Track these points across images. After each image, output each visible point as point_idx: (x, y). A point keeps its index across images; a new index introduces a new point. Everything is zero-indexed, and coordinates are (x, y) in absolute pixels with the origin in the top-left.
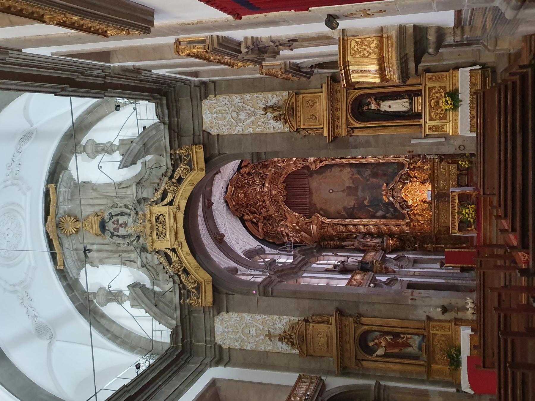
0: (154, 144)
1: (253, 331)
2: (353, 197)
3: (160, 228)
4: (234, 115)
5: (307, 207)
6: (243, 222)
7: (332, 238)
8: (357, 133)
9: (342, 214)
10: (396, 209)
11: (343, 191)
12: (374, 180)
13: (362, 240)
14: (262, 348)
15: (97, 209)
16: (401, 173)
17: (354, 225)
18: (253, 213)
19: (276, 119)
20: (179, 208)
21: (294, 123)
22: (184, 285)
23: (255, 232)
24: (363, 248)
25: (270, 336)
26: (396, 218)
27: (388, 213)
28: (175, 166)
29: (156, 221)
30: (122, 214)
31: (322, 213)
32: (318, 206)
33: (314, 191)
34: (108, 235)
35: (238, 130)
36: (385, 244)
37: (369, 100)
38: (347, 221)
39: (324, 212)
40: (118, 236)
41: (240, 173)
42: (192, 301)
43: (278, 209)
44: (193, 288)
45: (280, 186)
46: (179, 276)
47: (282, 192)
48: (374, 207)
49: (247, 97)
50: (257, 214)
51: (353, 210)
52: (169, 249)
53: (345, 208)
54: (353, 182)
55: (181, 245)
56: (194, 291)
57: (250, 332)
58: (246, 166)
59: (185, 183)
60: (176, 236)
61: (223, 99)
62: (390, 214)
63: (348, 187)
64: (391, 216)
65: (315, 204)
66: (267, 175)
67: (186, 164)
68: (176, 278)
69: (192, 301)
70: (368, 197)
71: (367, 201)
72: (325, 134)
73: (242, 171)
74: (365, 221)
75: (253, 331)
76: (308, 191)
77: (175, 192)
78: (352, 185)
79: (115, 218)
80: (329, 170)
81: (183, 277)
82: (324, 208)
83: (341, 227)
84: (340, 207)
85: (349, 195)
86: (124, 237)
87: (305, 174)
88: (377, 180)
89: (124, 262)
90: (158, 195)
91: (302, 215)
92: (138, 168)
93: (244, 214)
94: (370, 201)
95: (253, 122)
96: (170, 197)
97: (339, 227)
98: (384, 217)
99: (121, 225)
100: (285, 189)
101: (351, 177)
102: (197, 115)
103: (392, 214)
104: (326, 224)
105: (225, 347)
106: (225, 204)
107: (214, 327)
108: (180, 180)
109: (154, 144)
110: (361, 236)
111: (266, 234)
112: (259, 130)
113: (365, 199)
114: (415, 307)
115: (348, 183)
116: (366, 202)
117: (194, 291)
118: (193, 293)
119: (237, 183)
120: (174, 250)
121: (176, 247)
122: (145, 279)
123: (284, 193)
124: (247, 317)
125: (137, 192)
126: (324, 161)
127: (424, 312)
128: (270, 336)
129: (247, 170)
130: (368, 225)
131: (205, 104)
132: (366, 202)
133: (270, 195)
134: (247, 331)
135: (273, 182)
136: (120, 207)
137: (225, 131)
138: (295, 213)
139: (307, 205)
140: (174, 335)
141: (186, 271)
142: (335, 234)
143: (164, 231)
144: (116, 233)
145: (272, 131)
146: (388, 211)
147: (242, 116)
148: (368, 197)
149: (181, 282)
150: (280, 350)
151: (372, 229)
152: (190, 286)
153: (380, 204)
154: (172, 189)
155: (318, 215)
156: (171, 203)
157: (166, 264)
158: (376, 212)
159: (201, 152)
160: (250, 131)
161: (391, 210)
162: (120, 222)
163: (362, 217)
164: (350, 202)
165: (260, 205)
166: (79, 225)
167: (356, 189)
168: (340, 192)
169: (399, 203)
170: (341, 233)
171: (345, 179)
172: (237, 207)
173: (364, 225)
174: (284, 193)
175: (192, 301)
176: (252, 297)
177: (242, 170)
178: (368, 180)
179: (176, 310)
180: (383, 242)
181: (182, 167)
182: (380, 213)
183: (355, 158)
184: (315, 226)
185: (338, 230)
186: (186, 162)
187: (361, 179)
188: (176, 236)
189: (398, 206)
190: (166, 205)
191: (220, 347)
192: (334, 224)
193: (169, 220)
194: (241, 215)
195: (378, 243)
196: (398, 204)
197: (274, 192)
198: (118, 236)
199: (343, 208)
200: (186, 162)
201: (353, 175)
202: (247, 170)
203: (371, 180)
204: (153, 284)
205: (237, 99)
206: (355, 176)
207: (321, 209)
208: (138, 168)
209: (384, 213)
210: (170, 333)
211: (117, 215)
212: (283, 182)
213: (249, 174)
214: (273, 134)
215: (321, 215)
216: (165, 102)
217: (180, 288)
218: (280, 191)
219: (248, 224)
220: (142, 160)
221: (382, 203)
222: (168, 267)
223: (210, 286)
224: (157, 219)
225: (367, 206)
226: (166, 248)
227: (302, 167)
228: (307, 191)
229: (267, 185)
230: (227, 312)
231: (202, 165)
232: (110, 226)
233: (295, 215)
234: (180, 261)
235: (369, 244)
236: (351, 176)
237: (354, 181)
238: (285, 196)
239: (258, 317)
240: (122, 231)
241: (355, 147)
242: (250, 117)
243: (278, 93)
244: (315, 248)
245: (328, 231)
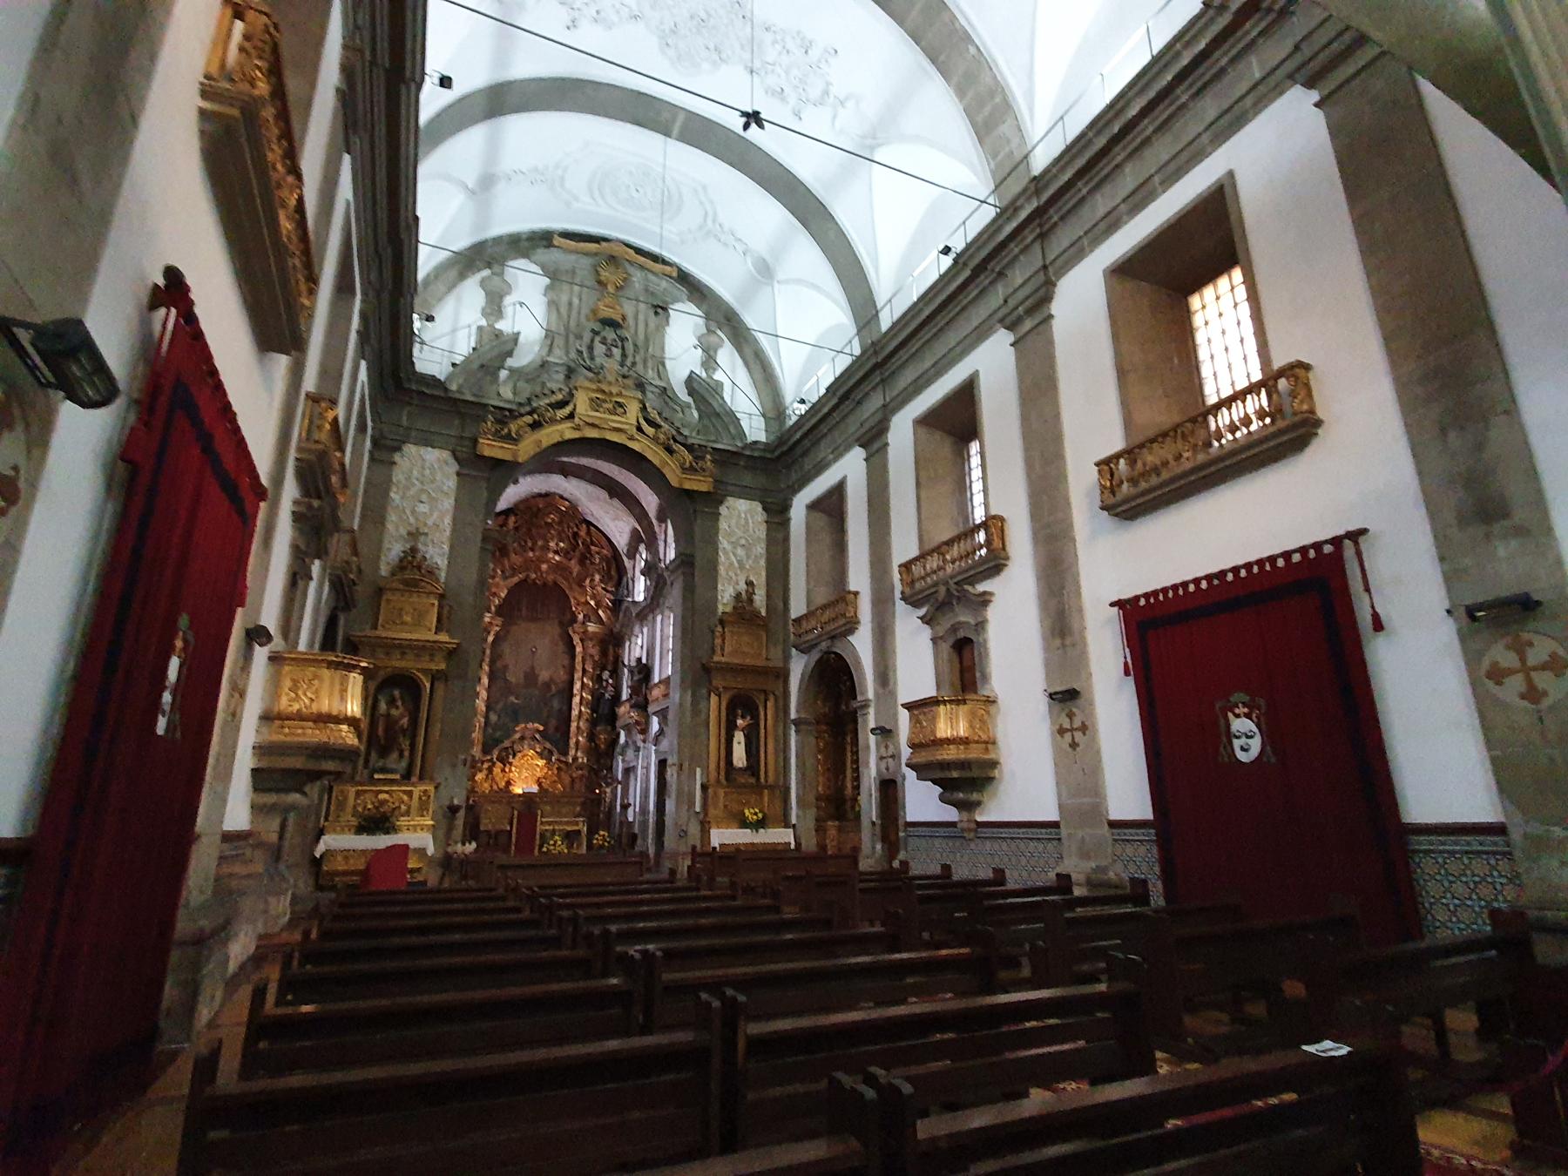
0: (714, 426)
1: (422, 508)
3: (606, 405)
4: (743, 542)
8: (714, 699)
10: (498, 742)
14: (392, 517)
15: (630, 321)
18: (516, 529)
19: (738, 596)
20: (631, 438)
21: (730, 619)
22: (516, 418)
25: (414, 535)
28: (690, 448)
29: (616, 402)
30: (624, 355)
32: (515, 628)
34: (597, 326)
35: (724, 543)
37: (749, 718)
40: (592, 341)
42: (489, 423)
44: (510, 431)
45: (550, 578)
46: (530, 413)
49: (763, 562)
52: (574, 409)
53: (506, 667)
55: (577, 428)
56: (506, 430)
57: (422, 502)
58: (589, 533)
59: (664, 455)
60: (593, 425)
61: (762, 532)
67: (690, 463)
68: (528, 409)
69: (489, 423)
72: (716, 658)
73: (584, 526)
75: (422, 508)
77: (655, 439)
79: (620, 344)
81: (528, 419)
85: (527, 676)
86: (591, 348)
89: (550, 335)
90: (654, 415)
92: (683, 395)
95: (731, 564)
96: (650, 431)
99: (610, 349)
102: (745, 493)
105: (397, 457)
106: (543, 492)
107: (433, 447)
108: (670, 450)
109: (714, 426)
112: (722, 570)
114: (454, 766)
115: (544, 675)
116: (512, 699)
117: (506, 430)
118: (502, 429)
120: (571, 416)
121: (576, 420)
122: (523, 358)
124: (448, 504)
125: (656, 387)
127: (446, 779)
128: (414, 535)
129: (583, 533)
131: (758, 507)
133: (541, 560)
134: (424, 497)
135: (558, 567)
136: (634, 357)
137: (723, 525)
140: (432, 381)
141: (536, 426)
143: (601, 410)
144: (597, 339)
145: (720, 587)
146: (496, 727)
147: (740, 551)
149: (522, 415)
150: (386, 545)
152: (513, 427)
154: (662, 436)
156: (639, 429)
157: (554, 399)
159: (704, 488)
160: (722, 558)
162: (615, 350)
164: (514, 676)
165: (526, 542)
166: (611, 289)
175: (489, 424)
176: (481, 517)
179: (474, 395)
181: (689, 457)
182: (493, 718)
186: (694, 464)
188: (593, 425)
189: (507, 744)
190: (638, 422)
191: (398, 449)
193: (615, 420)
197: (544, 567)
198: (592, 341)
200: (694, 464)
202: (583, 533)
204: (511, 370)
205: (760, 549)
206: (553, 687)
207: (508, 632)
208: (683, 395)
210: (438, 377)
211: (623, 348)
213: (576, 535)
214: (716, 588)
216: (769, 456)
217: (510, 411)
220: (693, 405)
222: (547, 401)
223: (508, 457)
224: (620, 405)
226: (575, 406)
229: (557, 558)
230: (458, 474)
231: (687, 486)
232: (610, 334)
234: (553, 421)
237: (547, 685)
239: (448, 520)
240: (599, 349)
241: (693, 695)
242: (738, 561)
243: (765, 603)
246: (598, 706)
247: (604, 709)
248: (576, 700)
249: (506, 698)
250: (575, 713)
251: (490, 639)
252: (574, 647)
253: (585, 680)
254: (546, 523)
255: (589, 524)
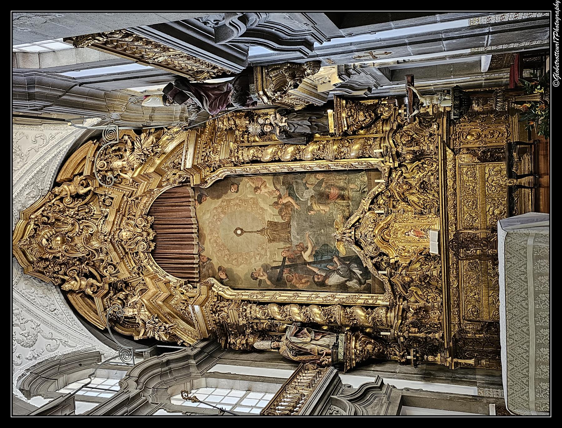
2: (282, 245)
5: (194, 264)
6: (65, 293)
7: (240, 331)
9: (261, 280)
10: (366, 272)
11: (261, 231)
12: (322, 207)
13: (294, 339)
16: (374, 192)
17: (281, 304)
23: (91, 317)
24: (296, 359)
26: (369, 290)
27: (350, 280)
31: (223, 276)
33: (206, 231)
36: (341, 350)
38: (268, 296)
39: (226, 275)
41: (56, 196)
43: (139, 269)
47: (145, 234)
48: (323, 265)
50: (94, 277)
51: (282, 272)
53: (266, 268)
54: (280, 212)
58: (70, 180)
62: (355, 281)
63: (272, 224)
64: (357, 286)
65: (208, 259)
66: (112, 198)
70: (309, 245)
71: (309, 252)
74: (303, 297)
76: (196, 231)
78: (278, 219)
80: (233, 189)
82: (225, 266)
83: (254, 307)
84: (257, 264)
87: (189, 197)
88: (327, 209)
91: (183, 281)
93: (66, 278)
94: (316, 254)
97: (251, 308)
98: (343, 288)
100: (152, 227)
101: (276, 203)
103: (360, 283)
104: (228, 300)
110: (293, 329)
111: (114, 321)
113: (305, 249)
116: (306, 256)
119: (43, 216)
123: (148, 234)
126: (220, 167)
129: (68, 189)
130: (307, 305)
132: (306, 256)
138: (170, 278)
139: (195, 261)
142: (242, 322)
146: (351, 275)
148: (309, 245)
151: (317, 315)
153: (335, 259)
155: (213, 281)
158: (327, 277)
161: (358, 272)
163: (300, 286)
165: (102, 261)
167: (288, 224)
168: (256, 234)
169: (372, 258)
170: (257, 321)
171: (266, 207)
172: (42, 265)
173: (301, 305)
174: (148, 234)
177: (57, 189)
178: (310, 209)
180: (336, 346)
182: (334, 279)
183: (279, 161)
184: (197, 308)
185: (248, 315)
187: (296, 207)
189: (369, 264)
192: (243, 301)
194: (60, 282)
195: (328, 346)
196: (369, 260)
199: (262, 266)
201: (280, 197)
202: (68, 189)
203: (315, 207)
207: (220, 269)
209: (344, 279)
212: (149, 214)
213: (76, 197)
215: (221, 281)
218: (139, 230)
219: (76, 299)
221: (338, 257)
225: (309, 263)
227: (180, 183)
228: (194, 231)
229: (111, 218)
233: (167, 283)
235: (308, 347)
236: (276, 200)
238: (153, 241)
244: (195, 356)
245: (228, 317)
246: (303, 135)
247: (303, 126)
248: (297, 166)
249: (306, 263)
250: (314, 165)
251: (228, 293)
252: (227, 178)
253: (268, 158)
254: (63, 242)
255: (56, 184)
